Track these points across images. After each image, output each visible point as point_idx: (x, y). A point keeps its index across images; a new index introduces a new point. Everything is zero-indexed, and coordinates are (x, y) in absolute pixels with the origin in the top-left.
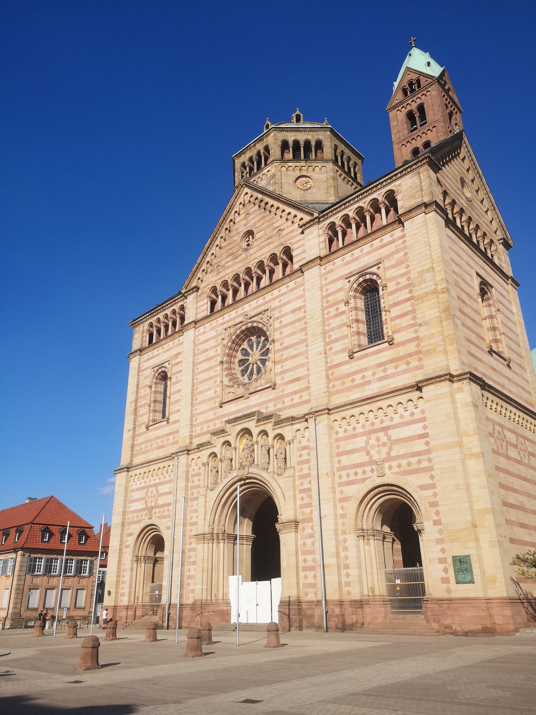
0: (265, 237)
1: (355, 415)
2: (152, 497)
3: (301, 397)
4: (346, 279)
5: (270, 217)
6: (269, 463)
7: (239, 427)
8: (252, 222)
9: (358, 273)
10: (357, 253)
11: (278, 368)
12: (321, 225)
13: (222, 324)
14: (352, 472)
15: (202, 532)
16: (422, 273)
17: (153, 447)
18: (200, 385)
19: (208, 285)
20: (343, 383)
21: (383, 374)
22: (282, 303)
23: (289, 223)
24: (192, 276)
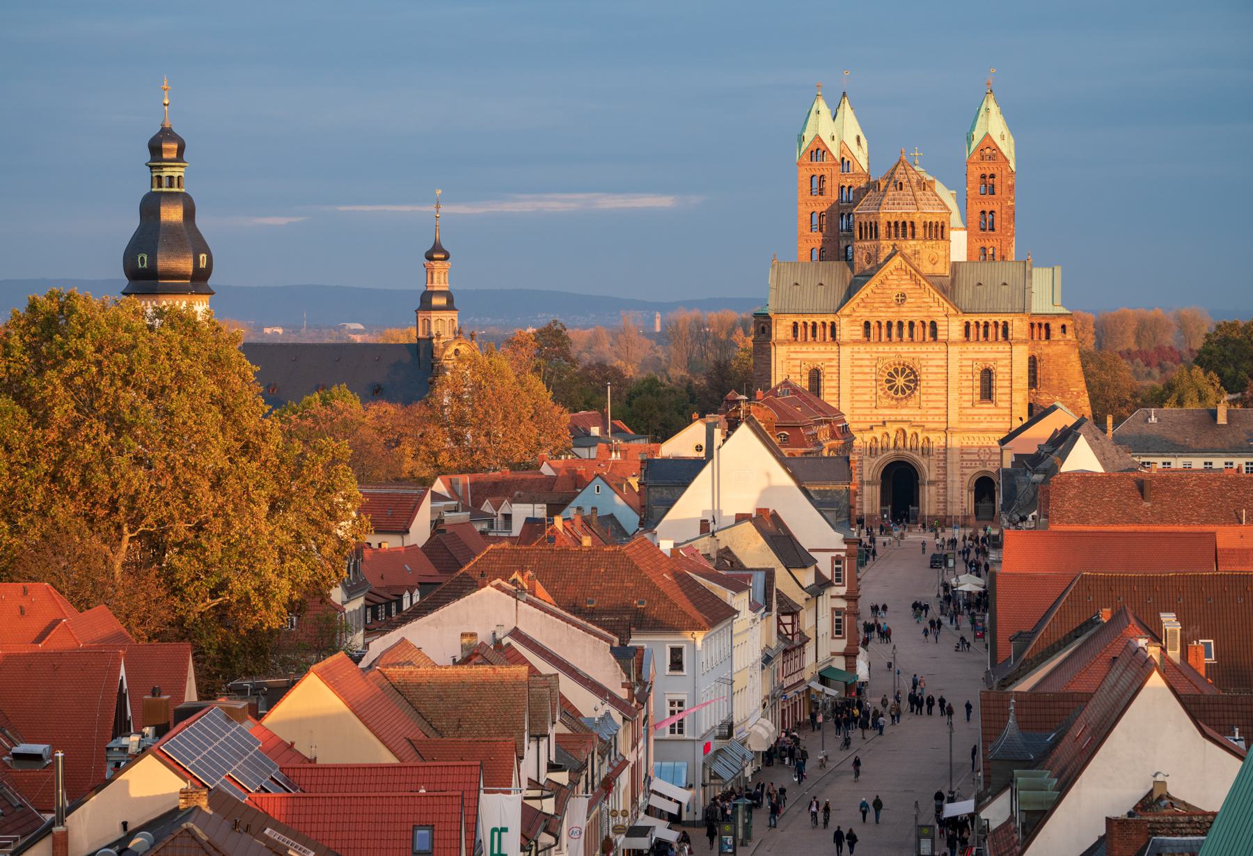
0: (915, 305)
8: (904, 287)
10: (982, 348)
12: (960, 318)
13: (876, 352)
14: (969, 463)
16: (1017, 378)
19: (860, 316)
23: (937, 305)
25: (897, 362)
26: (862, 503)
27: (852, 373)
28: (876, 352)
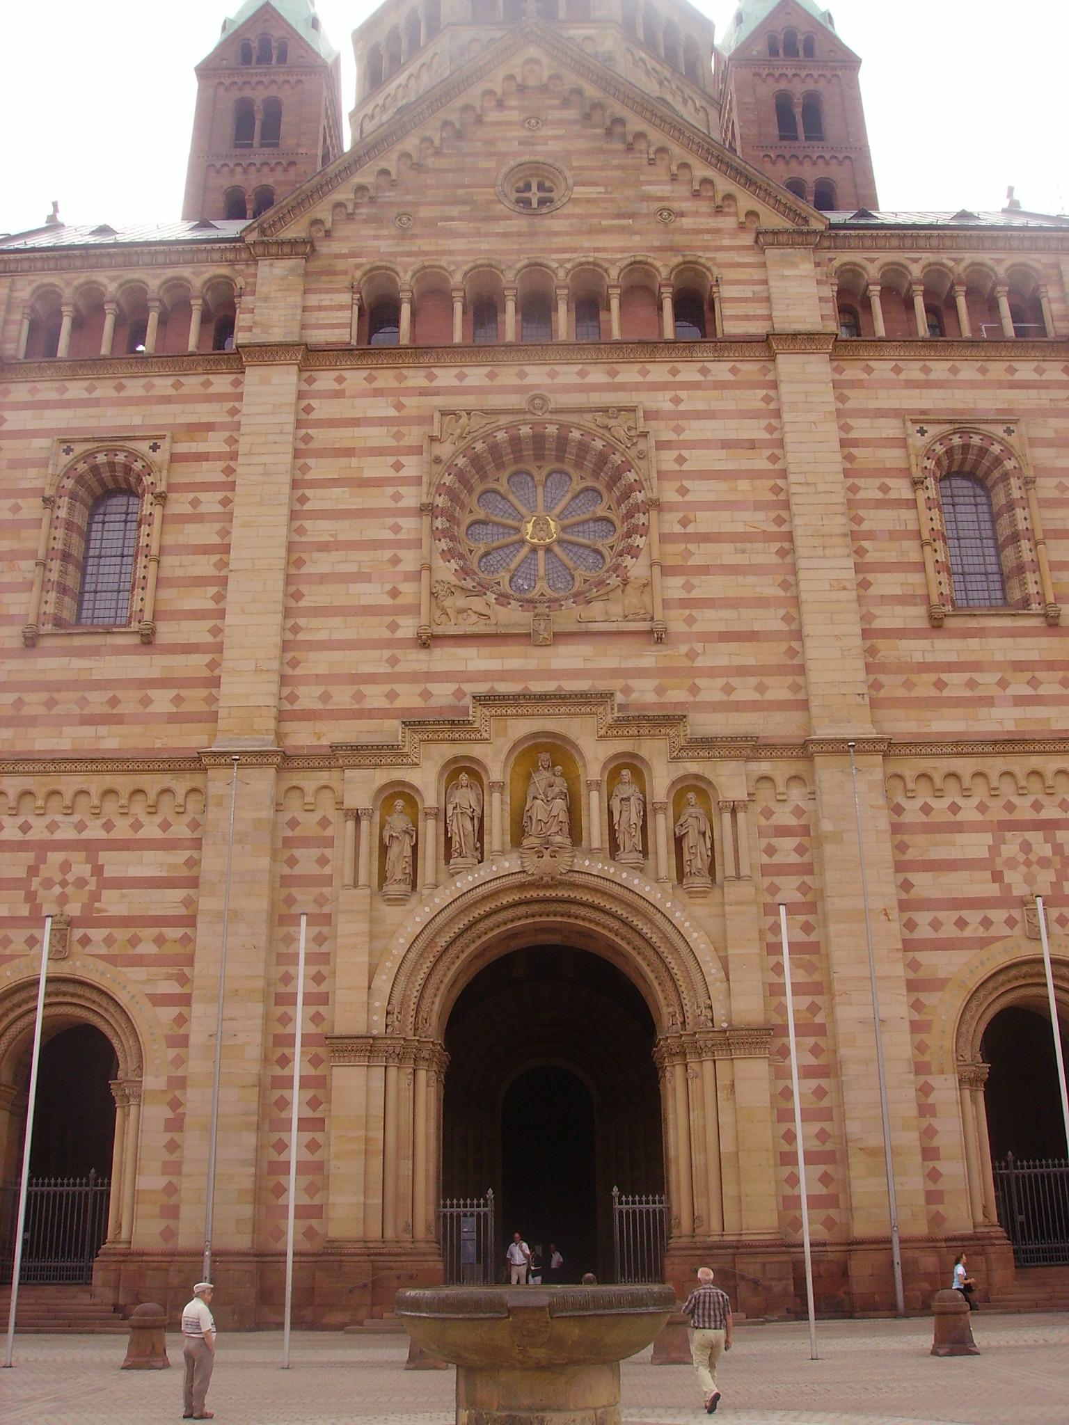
1: (960, 772)
2: (64, 884)
3: (761, 688)
4: (914, 422)
5: (629, 160)
6: (645, 852)
7: (521, 727)
8: (553, 147)
9: (951, 422)
10: (940, 369)
11: (674, 587)
13: (423, 392)
15: (361, 1029)
17: (56, 710)
18: (316, 555)
20: (909, 685)
21: (1029, 691)
22: (682, 407)
24: (294, 203)
25: (525, 430)
26: (315, 1170)
27: (295, 484)
28: (423, 392)
